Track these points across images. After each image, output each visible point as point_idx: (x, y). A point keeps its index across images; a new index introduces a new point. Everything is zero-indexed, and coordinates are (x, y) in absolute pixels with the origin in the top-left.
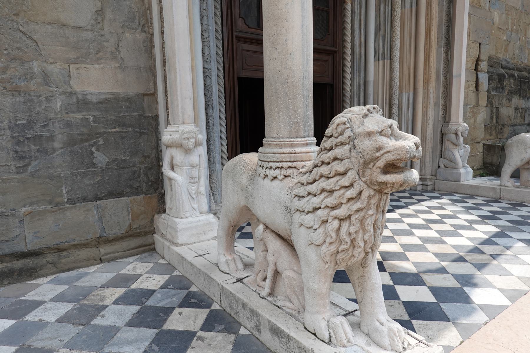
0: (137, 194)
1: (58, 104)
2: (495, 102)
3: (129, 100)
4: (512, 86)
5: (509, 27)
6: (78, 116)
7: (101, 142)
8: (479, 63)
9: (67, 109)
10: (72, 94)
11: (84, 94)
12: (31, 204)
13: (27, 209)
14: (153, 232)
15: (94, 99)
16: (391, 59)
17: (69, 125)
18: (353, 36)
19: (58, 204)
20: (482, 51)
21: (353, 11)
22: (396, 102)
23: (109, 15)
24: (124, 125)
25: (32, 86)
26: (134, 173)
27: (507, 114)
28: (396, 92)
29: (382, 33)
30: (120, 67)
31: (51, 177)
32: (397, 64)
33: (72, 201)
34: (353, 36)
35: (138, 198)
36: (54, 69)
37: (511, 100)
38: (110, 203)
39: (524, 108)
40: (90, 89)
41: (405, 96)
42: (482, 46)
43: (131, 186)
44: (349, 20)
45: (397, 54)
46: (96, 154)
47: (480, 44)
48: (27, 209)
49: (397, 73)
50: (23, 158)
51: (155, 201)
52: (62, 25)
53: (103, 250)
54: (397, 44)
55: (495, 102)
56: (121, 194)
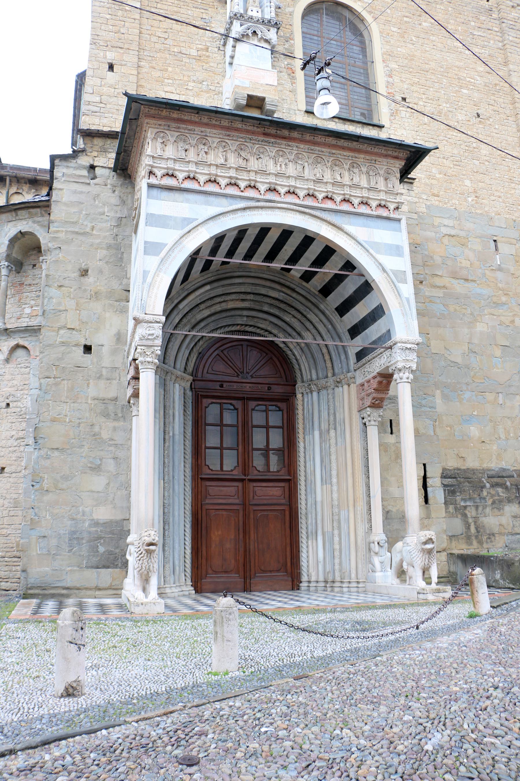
0: (116, 568)
1: (87, 524)
2: (471, 513)
3: (117, 522)
4: (501, 494)
5: (501, 436)
6: (94, 529)
7: (102, 541)
8: (428, 480)
9: (90, 526)
10: (93, 520)
11: (98, 520)
12: (71, 566)
13: (70, 568)
14: (122, 589)
15: (101, 522)
16: (331, 483)
17: (90, 533)
18: (305, 467)
19: (81, 568)
20: (427, 469)
21: (305, 448)
22: (336, 518)
23: (112, 485)
24: (113, 534)
25: (79, 517)
26: (116, 557)
27: (498, 523)
28: (336, 510)
29: (324, 464)
30: (114, 507)
31: (80, 555)
32: (335, 488)
33: (87, 567)
34: (305, 467)
35: (116, 570)
36: (87, 510)
37: (503, 509)
38: (103, 571)
40: (100, 517)
41: (342, 513)
42: (427, 466)
43: (113, 564)
44: (302, 454)
45: (334, 480)
46: (100, 547)
48: (70, 568)
49: (335, 496)
50: (71, 546)
51: (124, 573)
52: (92, 492)
53: (97, 593)
54: (334, 473)
55: (471, 513)
56: (108, 567)
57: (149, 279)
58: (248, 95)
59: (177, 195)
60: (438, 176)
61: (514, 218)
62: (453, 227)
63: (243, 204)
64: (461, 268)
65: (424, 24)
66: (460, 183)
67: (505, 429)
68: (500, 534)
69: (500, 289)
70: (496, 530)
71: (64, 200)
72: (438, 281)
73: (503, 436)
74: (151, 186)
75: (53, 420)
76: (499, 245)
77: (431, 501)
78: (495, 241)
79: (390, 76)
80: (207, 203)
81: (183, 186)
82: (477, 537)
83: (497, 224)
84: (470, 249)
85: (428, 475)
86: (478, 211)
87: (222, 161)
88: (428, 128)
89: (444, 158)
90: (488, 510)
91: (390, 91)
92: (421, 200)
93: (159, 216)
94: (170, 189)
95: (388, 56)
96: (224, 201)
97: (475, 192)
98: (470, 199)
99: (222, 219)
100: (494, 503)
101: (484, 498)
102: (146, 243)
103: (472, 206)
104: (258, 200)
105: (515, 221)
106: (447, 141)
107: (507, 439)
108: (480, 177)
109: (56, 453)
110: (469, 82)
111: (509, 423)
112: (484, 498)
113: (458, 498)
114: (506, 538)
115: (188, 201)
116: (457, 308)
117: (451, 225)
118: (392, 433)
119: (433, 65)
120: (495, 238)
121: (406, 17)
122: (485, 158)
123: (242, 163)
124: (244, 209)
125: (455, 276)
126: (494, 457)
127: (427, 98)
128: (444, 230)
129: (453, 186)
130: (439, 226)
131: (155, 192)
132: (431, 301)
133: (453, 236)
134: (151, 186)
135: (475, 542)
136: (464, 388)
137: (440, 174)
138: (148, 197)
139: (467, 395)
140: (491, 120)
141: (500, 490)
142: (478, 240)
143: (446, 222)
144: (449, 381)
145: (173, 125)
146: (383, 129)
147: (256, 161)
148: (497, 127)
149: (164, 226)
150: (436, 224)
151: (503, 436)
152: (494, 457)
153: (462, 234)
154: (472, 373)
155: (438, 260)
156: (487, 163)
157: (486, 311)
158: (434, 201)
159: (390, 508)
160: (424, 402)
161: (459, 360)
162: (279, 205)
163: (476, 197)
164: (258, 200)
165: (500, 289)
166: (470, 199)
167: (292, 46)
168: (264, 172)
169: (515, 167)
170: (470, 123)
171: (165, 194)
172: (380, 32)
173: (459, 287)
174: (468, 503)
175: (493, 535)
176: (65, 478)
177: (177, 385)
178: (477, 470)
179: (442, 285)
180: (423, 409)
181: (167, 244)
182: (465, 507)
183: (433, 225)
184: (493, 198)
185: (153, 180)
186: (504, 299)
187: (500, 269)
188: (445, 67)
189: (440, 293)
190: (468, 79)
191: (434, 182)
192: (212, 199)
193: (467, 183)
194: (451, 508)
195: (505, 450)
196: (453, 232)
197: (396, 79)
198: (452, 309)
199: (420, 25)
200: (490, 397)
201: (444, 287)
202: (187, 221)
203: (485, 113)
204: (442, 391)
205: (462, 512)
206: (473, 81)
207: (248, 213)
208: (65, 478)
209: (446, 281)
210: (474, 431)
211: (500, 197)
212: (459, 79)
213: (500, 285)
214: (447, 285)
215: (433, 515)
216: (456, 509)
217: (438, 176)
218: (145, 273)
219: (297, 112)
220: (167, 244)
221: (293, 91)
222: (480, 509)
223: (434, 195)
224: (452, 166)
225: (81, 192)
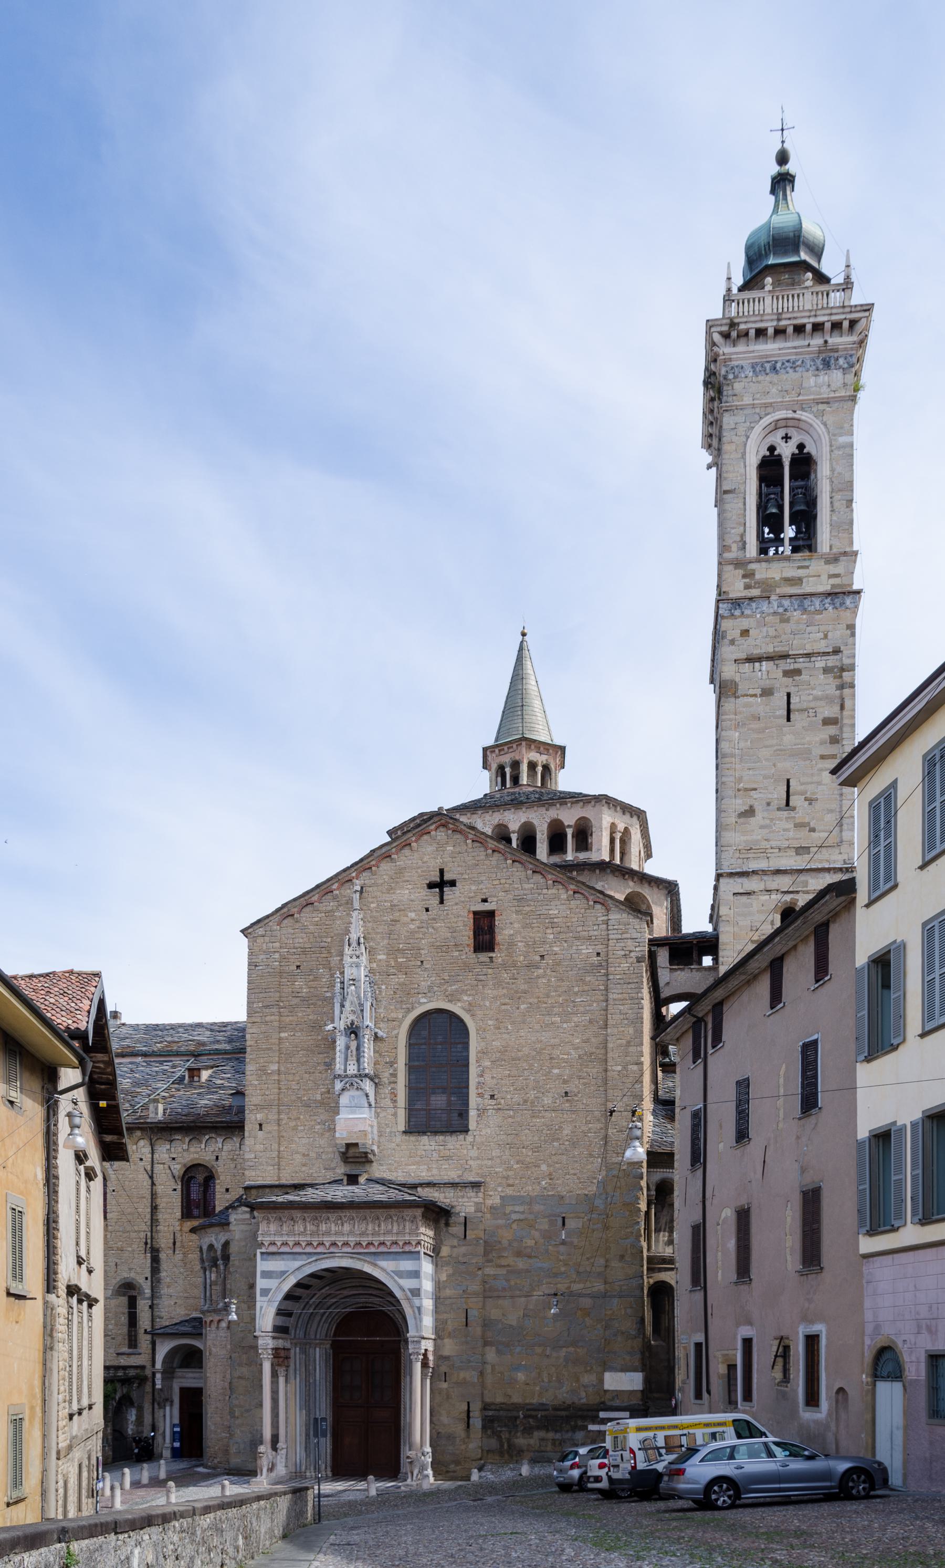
39: (558, 1439)
47: (468, 1403)
57: (262, 1312)
58: (346, 1144)
59: (277, 1257)
60: (515, 1166)
61: (586, 1193)
62: (523, 1213)
63: (314, 1259)
64: (525, 1248)
65: (522, 1007)
66: (537, 1169)
67: (549, 1374)
68: (528, 1450)
69: (561, 1261)
70: (525, 1448)
71: (237, 1237)
72: (504, 1262)
73: (546, 1380)
74: (262, 1253)
75: (239, 1377)
76: (566, 1220)
77: (471, 1427)
78: (564, 1218)
79: (482, 1076)
80: (295, 1260)
81: (280, 1251)
82: (508, 1452)
83: (567, 1202)
84: (536, 1230)
85: (471, 1409)
86: (550, 1193)
87: (302, 1230)
88: (513, 1120)
89: (523, 1148)
90: (519, 1434)
91: (480, 1091)
92: (496, 1193)
93: (268, 1271)
94: (273, 1253)
95: (483, 1053)
96: (304, 1256)
97: (550, 1174)
98: (543, 1183)
99: (304, 1269)
100: (525, 1429)
101: (517, 1426)
102: (261, 1289)
103: (545, 1188)
104: (325, 1253)
105: (587, 1195)
106: (529, 1130)
107: (550, 1382)
108: (555, 1158)
109: (242, 1397)
110: (563, 1059)
111: (554, 1369)
112: (517, 1426)
113: (496, 1425)
114: (532, 1454)
115: (283, 1260)
116: (518, 1282)
117: (522, 1210)
118: (445, 1381)
119: (526, 1050)
120: (564, 1215)
121: (504, 1004)
122: (566, 1138)
123: (314, 1228)
124: (316, 1260)
125: (519, 1254)
126: (536, 1395)
127: (516, 1089)
128: (514, 1217)
129: (529, 1172)
130: (509, 1214)
131: (265, 1256)
132: (494, 1279)
133: (522, 1220)
134: (262, 1253)
135: (506, 1456)
136: (516, 1344)
137: (517, 1163)
138: (262, 1260)
139: (518, 1349)
140: (580, 1095)
141: (531, 1420)
142: (546, 1220)
143: (517, 1208)
144: (504, 1339)
145: (272, 1211)
146: (469, 1133)
147: (324, 1226)
148: (585, 1102)
149: (271, 1277)
150: (507, 1212)
151: (546, 1380)
152: (536, 1395)
153: (531, 1217)
154: (525, 1333)
155: (505, 1242)
156: (567, 1143)
157: (544, 1282)
158: (509, 1191)
159: (440, 1430)
160: (472, 1359)
161: (514, 1323)
162: (337, 1255)
163: (550, 1179)
164: (325, 1253)
165: (561, 1261)
166: (544, 1183)
167: (395, 1070)
168: (328, 1233)
169: (597, 1140)
170: (556, 1105)
171: (270, 1257)
172: (477, 1030)
173: (521, 1264)
174: (503, 1429)
175: (522, 1451)
176: (248, 1411)
177: (318, 1349)
178: (519, 1404)
179: (506, 1264)
180: (471, 1364)
181: (271, 1289)
182: (501, 1431)
183: (505, 1214)
184: (568, 1177)
185: (263, 1250)
186: (563, 1269)
187: (563, 1243)
188: (538, 1050)
189: (503, 1271)
190: (561, 1056)
191: (511, 1173)
192: (297, 1256)
193: (544, 1167)
194: (489, 1432)
195: (547, 1390)
196: (522, 1217)
197: (487, 1077)
198: (513, 1283)
199: (518, 1008)
200: (538, 1350)
201: (508, 1266)
202: (283, 1273)
203: (575, 1090)
204: (497, 1348)
205: (498, 1435)
206: (566, 1057)
207: (319, 1262)
208: (248, 1411)
209: (510, 1260)
210: (521, 1376)
211: (575, 1174)
212: (551, 1058)
213: (561, 1258)
214: (512, 1263)
215: (472, 1436)
216: (493, 1433)
217: (515, 1166)
218: (261, 1308)
219: (397, 1133)
220: (271, 1289)
221: (395, 1115)
222: (513, 1433)
223: (509, 1185)
224: (530, 1153)
225: (246, 1231)
